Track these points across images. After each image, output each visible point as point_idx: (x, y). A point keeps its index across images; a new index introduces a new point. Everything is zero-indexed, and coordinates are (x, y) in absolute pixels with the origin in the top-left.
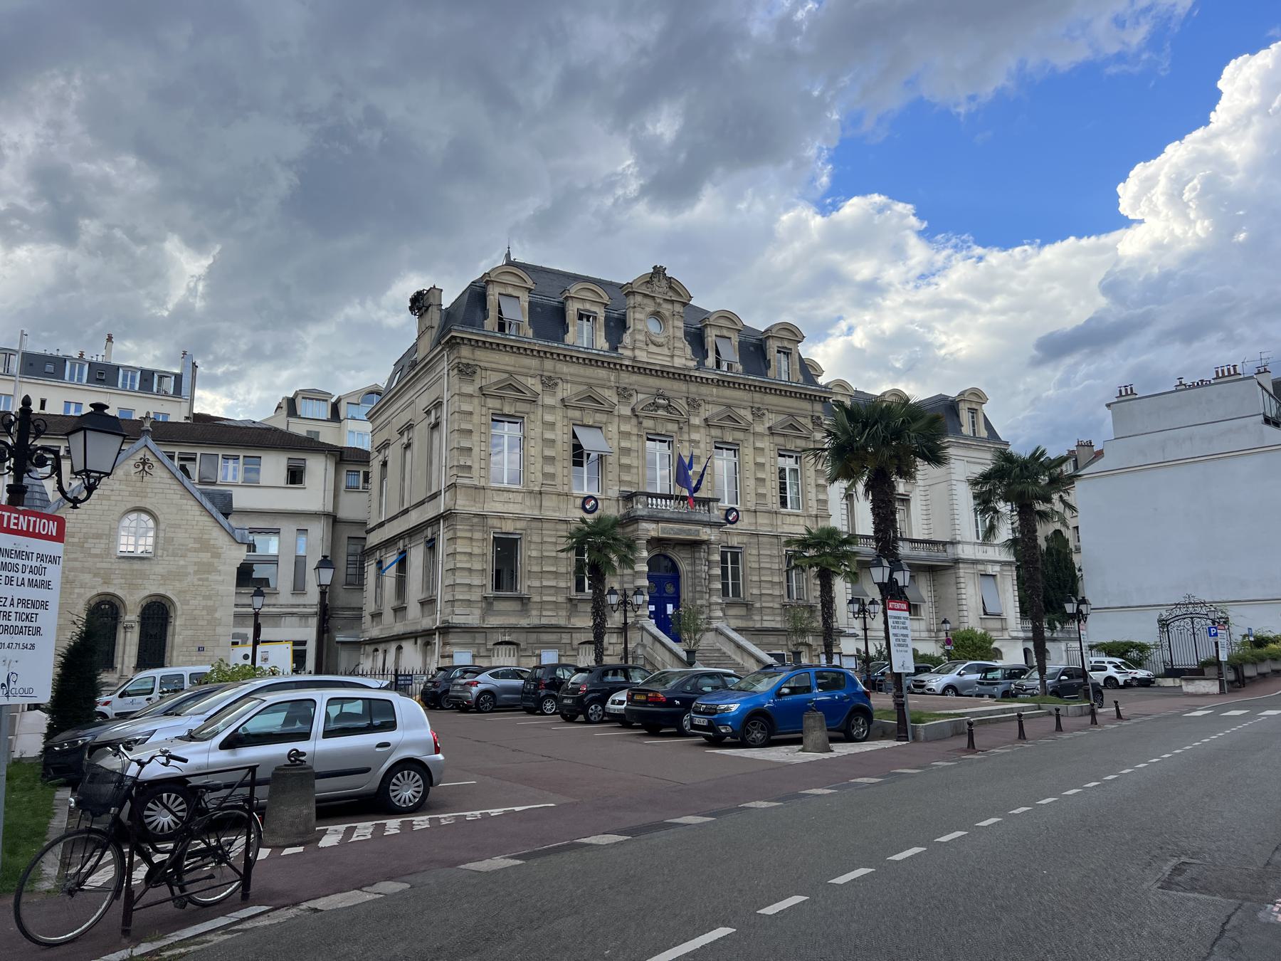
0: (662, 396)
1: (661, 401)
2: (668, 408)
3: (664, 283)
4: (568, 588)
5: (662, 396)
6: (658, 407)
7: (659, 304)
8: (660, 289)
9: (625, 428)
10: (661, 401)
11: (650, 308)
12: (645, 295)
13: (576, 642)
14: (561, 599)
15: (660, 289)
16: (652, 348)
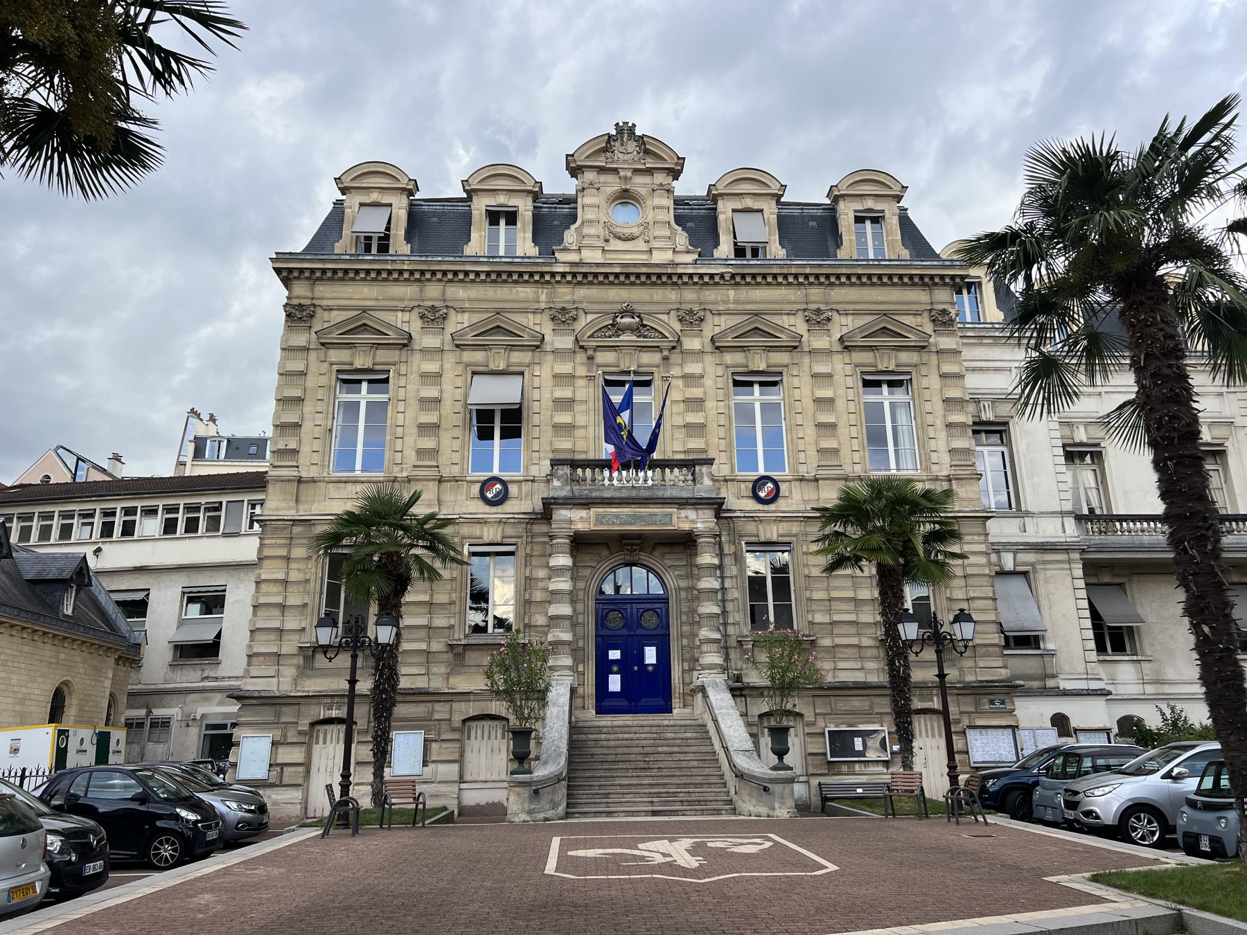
0: (629, 312)
1: (627, 320)
2: (640, 329)
3: (632, 146)
4: (451, 627)
5: (632, 314)
6: (618, 330)
7: (626, 179)
8: (626, 155)
9: (565, 368)
10: (627, 320)
11: (612, 185)
12: (601, 170)
13: (457, 719)
14: (437, 646)
15: (626, 155)
16: (616, 245)
